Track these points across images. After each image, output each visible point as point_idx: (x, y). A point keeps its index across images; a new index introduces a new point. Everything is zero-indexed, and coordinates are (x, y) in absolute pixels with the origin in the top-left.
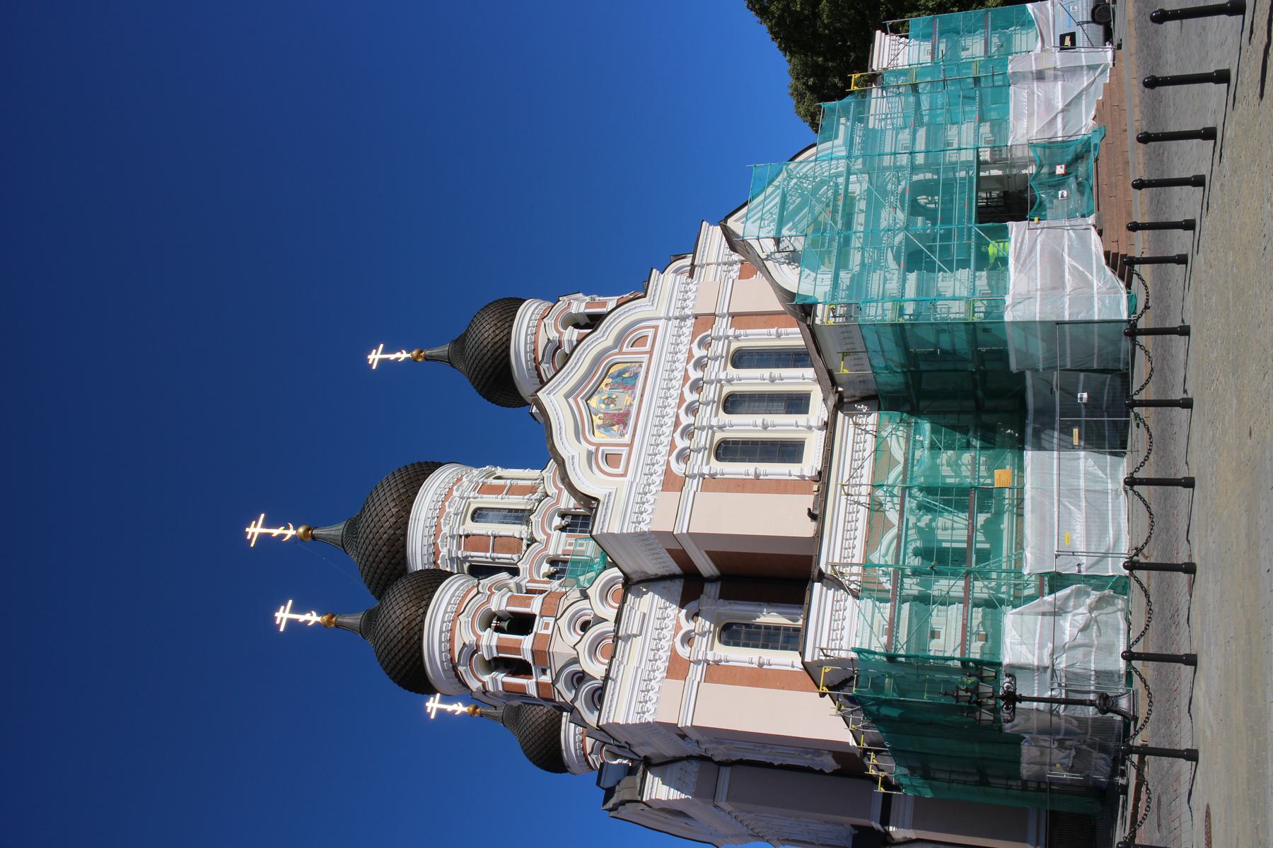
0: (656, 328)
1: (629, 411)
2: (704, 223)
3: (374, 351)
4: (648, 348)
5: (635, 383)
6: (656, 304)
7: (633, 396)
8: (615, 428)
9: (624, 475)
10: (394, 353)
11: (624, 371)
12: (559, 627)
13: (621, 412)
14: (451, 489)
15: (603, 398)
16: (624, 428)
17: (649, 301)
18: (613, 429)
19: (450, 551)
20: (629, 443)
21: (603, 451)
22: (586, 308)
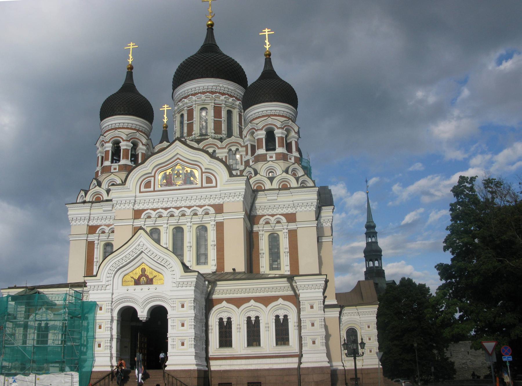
0: (216, 186)
1: (173, 185)
3: (270, 30)
4: (205, 185)
7: (181, 185)
8: (165, 181)
9: (140, 192)
10: (269, 41)
11: (194, 177)
12: (110, 175)
13: (173, 182)
14: (216, 92)
15: (181, 172)
16: (164, 185)
17: (227, 180)
18: (164, 180)
19: (186, 103)
20: (155, 190)
21: (152, 179)
22: (278, 137)
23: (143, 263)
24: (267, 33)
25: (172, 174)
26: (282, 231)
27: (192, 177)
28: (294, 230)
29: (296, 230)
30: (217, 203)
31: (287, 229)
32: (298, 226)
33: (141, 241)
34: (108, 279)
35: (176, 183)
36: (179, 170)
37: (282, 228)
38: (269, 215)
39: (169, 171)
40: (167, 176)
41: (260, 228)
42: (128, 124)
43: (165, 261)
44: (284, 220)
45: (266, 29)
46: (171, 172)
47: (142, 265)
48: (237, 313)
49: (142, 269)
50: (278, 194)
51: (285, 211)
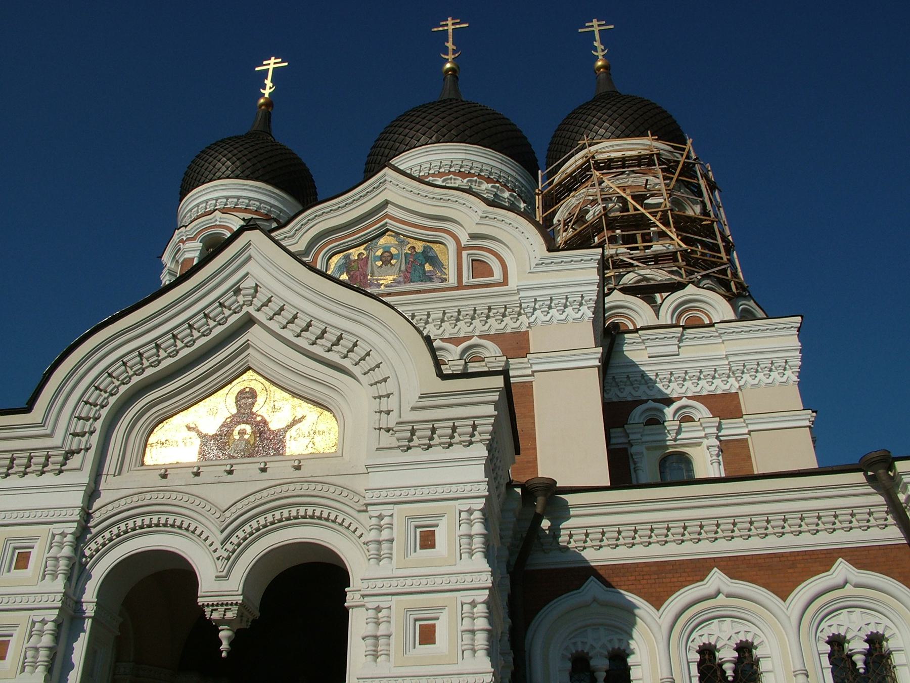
2: (799, 319)
5: (414, 282)
6: (541, 269)
13: (369, 277)
15: (394, 251)
18: (343, 274)
23: (249, 368)
24: (596, 30)
25: (367, 258)
26: (699, 444)
27: (427, 264)
28: (737, 440)
29: (746, 440)
30: (508, 331)
31: (717, 437)
32: (751, 427)
33: (247, 274)
34: (79, 426)
35: (377, 280)
36: (389, 247)
37: (702, 434)
38: (655, 400)
39: (361, 249)
40: (353, 264)
41: (631, 437)
42: (250, 201)
43: (347, 343)
44: (702, 412)
45: (595, 21)
46: (364, 252)
47: (245, 376)
48: (655, 628)
49: (241, 392)
50: (680, 340)
51: (705, 388)
